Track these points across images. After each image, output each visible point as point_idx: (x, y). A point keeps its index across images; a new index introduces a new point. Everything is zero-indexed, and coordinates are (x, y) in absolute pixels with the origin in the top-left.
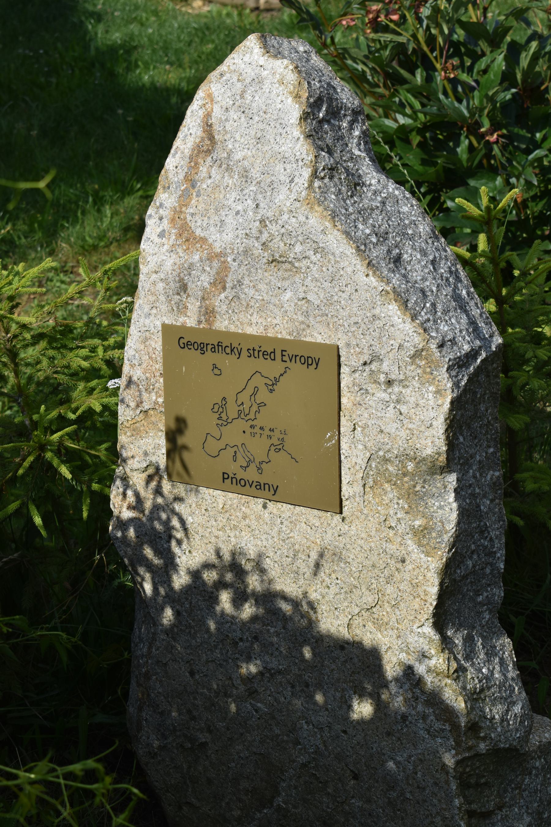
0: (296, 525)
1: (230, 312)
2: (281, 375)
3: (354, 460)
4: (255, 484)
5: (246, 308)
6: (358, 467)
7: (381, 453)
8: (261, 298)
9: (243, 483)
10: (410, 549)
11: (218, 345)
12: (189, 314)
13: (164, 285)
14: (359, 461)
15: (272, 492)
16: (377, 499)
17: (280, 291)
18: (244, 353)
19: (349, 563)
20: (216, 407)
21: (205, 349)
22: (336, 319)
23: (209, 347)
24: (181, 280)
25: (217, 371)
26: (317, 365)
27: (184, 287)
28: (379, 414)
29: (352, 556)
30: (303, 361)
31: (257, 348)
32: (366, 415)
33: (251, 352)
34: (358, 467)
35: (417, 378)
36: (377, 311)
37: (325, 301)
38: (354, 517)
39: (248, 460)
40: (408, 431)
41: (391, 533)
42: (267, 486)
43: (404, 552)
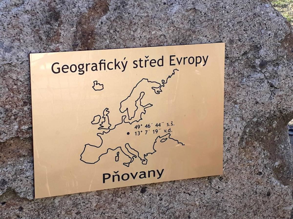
0: (175, 197)
1: (112, 31)
2: (169, 77)
3: (234, 130)
4: (139, 174)
5: (130, 25)
6: (236, 135)
7: (255, 120)
8: (146, 14)
9: (125, 177)
10: (274, 184)
11: (100, 63)
12: (62, 40)
13: (30, 16)
14: (238, 130)
15: (157, 175)
16: (247, 156)
17: (166, 6)
18: (130, 65)
19: (226, 211)
20: (97, 119)
21: (84, 69)
22: (221, 22)
23: (90, 67)
24: (52, 9)
25: (97, 87)
26: (205, 62)
27: (55, 16)
28: (255, 90)
29: (229, 205)
30: (191, 61)
31: (144, 59)
32: (244, 93)
33: (138, 63)
34: (236, 135)
35: (285, 57)
36: (258, 10)
37: (211, 8)
38: (230, 174)
39: (131, 156)
40: (278, 98)
41: (259, 177)
42: (152, 173)
43: (269, 188)
